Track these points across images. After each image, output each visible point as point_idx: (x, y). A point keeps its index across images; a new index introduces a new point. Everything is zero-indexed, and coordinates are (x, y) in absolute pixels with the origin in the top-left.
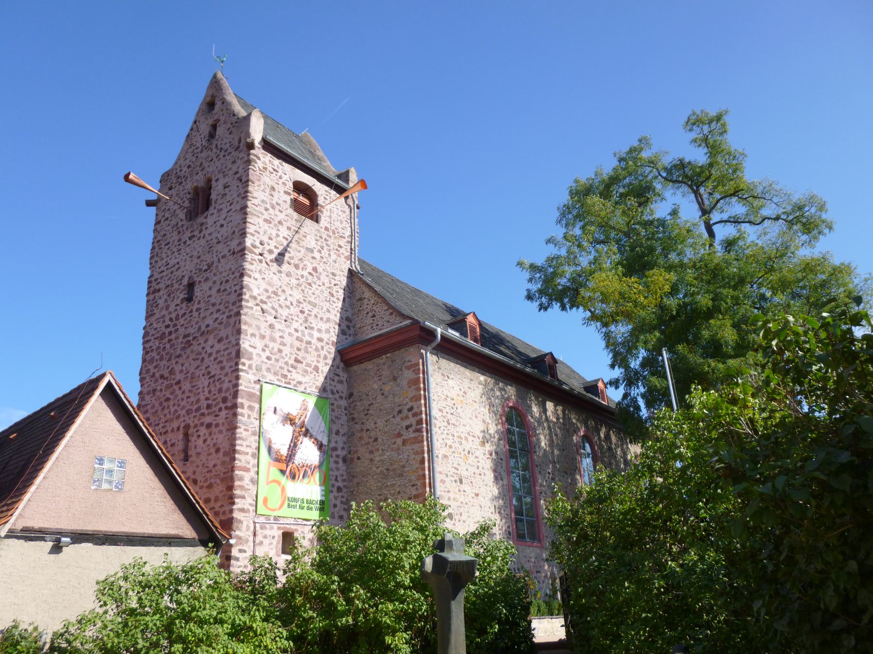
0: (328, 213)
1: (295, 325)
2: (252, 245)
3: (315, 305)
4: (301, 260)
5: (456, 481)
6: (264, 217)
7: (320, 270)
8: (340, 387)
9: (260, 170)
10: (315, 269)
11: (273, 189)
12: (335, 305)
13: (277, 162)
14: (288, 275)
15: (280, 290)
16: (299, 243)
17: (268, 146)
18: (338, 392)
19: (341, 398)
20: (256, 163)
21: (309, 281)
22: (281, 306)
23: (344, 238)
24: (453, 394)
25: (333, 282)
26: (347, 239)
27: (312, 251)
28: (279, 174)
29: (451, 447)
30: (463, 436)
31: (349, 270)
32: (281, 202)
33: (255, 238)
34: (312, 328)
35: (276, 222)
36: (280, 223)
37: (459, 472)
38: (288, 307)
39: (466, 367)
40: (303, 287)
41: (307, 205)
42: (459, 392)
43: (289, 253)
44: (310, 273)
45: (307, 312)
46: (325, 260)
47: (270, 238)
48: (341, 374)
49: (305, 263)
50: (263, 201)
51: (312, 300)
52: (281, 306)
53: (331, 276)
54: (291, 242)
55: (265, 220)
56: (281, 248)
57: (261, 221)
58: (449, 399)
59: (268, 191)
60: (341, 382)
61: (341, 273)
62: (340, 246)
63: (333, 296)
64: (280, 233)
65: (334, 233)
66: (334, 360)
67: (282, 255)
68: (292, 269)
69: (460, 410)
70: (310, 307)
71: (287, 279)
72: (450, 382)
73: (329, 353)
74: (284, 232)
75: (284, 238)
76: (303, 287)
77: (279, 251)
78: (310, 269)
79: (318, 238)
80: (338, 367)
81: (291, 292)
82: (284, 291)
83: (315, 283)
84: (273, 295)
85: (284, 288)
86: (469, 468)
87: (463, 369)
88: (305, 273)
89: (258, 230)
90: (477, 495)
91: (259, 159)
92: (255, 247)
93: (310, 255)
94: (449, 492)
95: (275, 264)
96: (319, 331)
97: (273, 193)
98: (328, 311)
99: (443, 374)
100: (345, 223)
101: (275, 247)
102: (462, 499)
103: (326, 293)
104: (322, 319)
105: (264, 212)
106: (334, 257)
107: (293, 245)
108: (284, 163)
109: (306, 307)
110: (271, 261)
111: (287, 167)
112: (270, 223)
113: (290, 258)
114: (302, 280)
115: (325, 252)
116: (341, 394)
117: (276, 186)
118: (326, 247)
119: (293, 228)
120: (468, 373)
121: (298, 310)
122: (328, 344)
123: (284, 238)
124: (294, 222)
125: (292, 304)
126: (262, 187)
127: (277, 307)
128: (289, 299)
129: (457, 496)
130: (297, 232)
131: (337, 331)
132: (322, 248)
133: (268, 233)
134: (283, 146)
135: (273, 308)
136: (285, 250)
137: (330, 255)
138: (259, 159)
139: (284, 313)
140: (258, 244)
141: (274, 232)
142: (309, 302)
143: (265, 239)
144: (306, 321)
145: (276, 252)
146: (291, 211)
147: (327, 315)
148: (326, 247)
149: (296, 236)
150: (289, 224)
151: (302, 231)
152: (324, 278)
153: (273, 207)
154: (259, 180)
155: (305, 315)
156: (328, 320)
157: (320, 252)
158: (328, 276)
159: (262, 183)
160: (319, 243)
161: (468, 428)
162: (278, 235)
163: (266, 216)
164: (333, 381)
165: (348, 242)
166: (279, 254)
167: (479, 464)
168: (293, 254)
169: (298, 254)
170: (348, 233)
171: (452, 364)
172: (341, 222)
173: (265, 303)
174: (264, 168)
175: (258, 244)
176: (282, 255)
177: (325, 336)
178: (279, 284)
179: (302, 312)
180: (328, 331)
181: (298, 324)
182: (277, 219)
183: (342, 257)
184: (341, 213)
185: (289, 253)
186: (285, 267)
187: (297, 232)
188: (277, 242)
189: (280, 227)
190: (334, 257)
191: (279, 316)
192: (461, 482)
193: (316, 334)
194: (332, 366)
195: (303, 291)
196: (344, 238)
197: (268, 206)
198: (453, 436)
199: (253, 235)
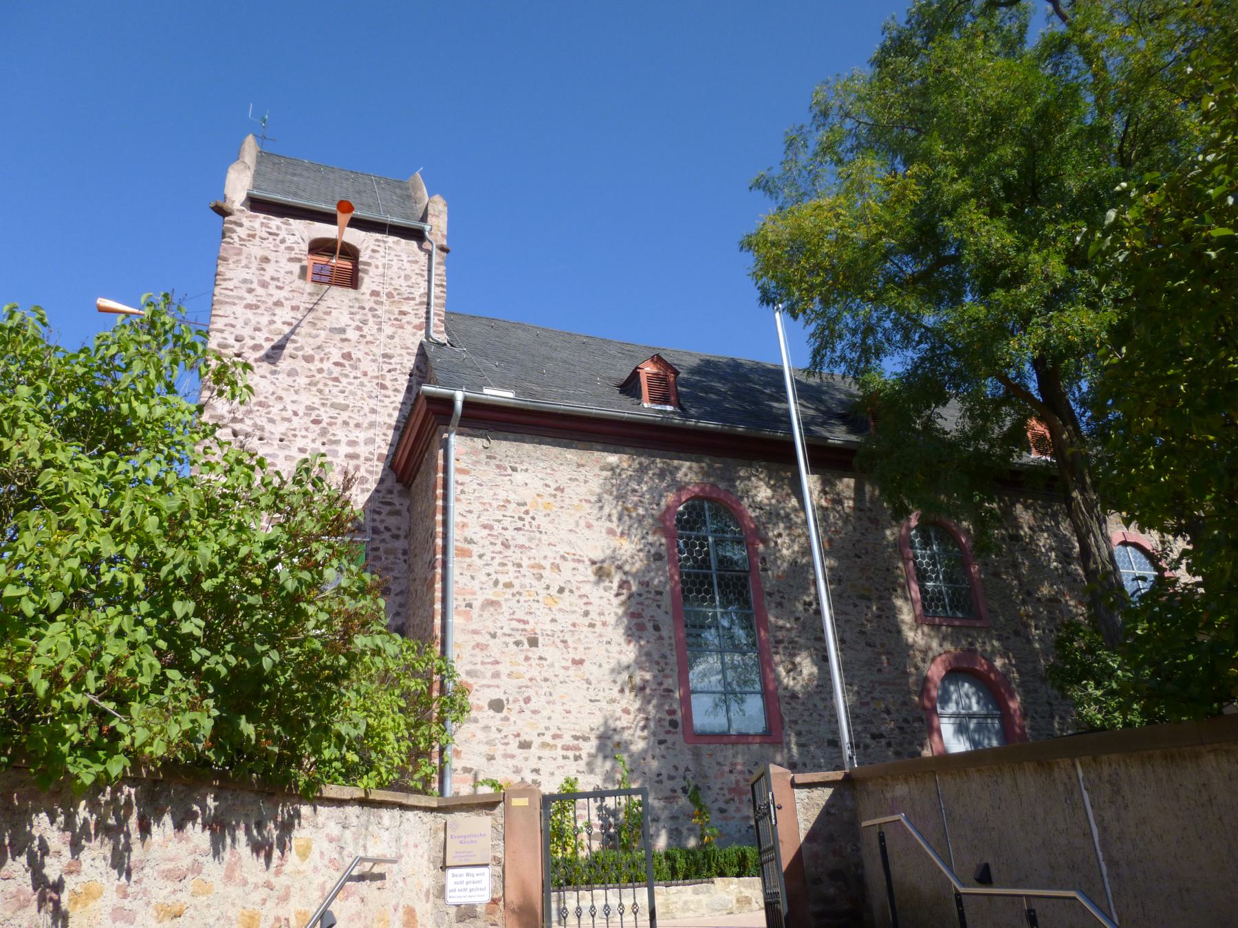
0: (381, 270)
1: (300, 443)
2: (219, 345)
3: (345, 408)
4: (319, 347)
5: (517, 643)
6: (245, 302)
7: (356, 354)
8: (392, 521)
9: (241, 239)
10: (347, 356)
11: (266, 260)
12: (387, 401)
13: (275, 222)
14: (292, 373)
15: (273, 398)
16: (315, 324)
17: (256, 204)
18: (387, 529)
19: (396, 537)
20: (234, 231)
21: (334, 375)
22: (271, 421)
23: (414, 299)
24: (527, 495)
25: (386, 367)
26: (418, 300)
27: (343, 331)
28: (280, 237)
29: (508, 585)
30: (547, 564)
31: (421, 344)
32: (281, 275)
33: (226, 335)
34: (337, 442)
35: (270, 303)
36: (278, 304)
37: (527, 627)
38: (289, 420)
39: (568, 446)
40: (320, 386)
41: (338, 266)
42: (542, 490)
43: (294, 341)
44: (336, 364)
45: (326, 420)
46: (369, 338)
47: (257, 329)
48: (396, 500)
49: (327, 350)
50: (245, 281)
51: (340, 400)
52: (271, 421)
53: (381, 360)
54: (298, 326)
55: (249, 306)
56: (277, 339)
57: (239, 310)
58: (513, 506)
59: (255, 264)
60: (398, 513)
61: (404, 352)
62: (403, 313)
63: (383, 387)
64: (275, 318)
65: (390, 295)
66: (381, 481)
67: (279, 348)
68: (299, 364)
69: (541, 520)
70: (333, 412)
71: (289, 381)
72: (519, 477)
73: (371, 472)
74: (285, 314)
75: (284, 323)
76: (320, 386)
77: (272, 343)
78: (336, 356)
79: (355, 310)
80: (390, 492)
81: (295, 397)
82: (281, 398)
83: (346, 376)
84: (256, 408)
85: (280, 393)
86: (559, 616)
87: (556, 450)
88: (326, 365)
89: (233, 322)
90: (578, 662)
91: (241, 225)
92: (226, 346)
93: (338, 337)
94: (497, 663)
95: (265, 365)
96: (352, 443)
97: (264, 265)
98: (373, 411)
99: (498, 467)
100: (414, 277)
101: (267, 339)
102: (534, 672)
103: (371, 386)
104: (357, 425)
105: (247, 295)
106: (388, 330)
107: (303, 330)
108: (291, 221)
109: (325, 414)
110: (256, 360)
111: (297, 225)
112: (257, 307)
113: (296, 349)
114: (318, 376)
115: (370, 328)
116: (395, 531)
117: (272, 256)
118: (371, 320)
119: (302, 306)
120: (571, 455)
121: (307, 420)
122: (367, 459)
123: (284, 323)
124: (305, 297)
125: (295, 414)
126: (244, 262)
127: (262, 421)
128: (290, 407)
129: (522, 669)
130: (310, 310)
131: (389, 439)
132: (365, 322)
133: (253, 322)
134: (279, 197)
135: (255, 425)
136: (287, 338)
137: (380, 330)
138: (241, 225)
139: (280, 429)
140: (231, 341)
141: (264, 320)
142: (333, 406)
143: (246, 332)
144: (324, 432)
145: (267, 346)
146: (299, 283)
147: (373, 417)
148: (371, 320)
149: (310, 317)
150: (294, 303)
151: (322, 307)
152: (366, 365)
153: (264, 285)
154: (239, 253)
155: (324, 424)
156: (372, 425)
157: (359, 328)
158: (374, 361)
159: (243, 257)
160: (358, 317)
161: (563, 549)
162: (272, 322)
163: (250, 299)
164: (379, 513)
165: (421, 303)
166: (273, 348)
167: (589, 608)
168: (304, 341)
169: (311, 341)
170: (423, 288)
171: (527, 447)
172: (407, 277)
173: (242, 421)
174: (249, 235)
175: (231, 341)
176: (279, 348)
177: (363, 450)
178: (271, 389)
179: (316, 422)
180: (369, 441)
181: (309, 440)
182: (270, 302)
183: (409, 329)
184: (407, 265)
185: (294, 341)
186: (284, 364)
187: (310, 310)
188: (270, 332)
189: (278, 311)
190: (388, 330)
191: (266, 435)
192: (533, 642)
193: (343, 449)
194: (377, 491)
195: (320, 391)
196: (414, 299)
197: (255, 286)
198: (519, 566)
199: (222, 331)
